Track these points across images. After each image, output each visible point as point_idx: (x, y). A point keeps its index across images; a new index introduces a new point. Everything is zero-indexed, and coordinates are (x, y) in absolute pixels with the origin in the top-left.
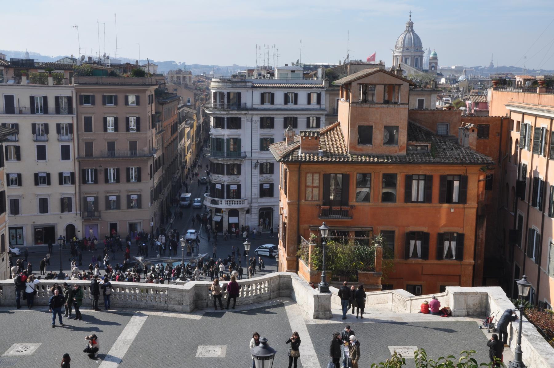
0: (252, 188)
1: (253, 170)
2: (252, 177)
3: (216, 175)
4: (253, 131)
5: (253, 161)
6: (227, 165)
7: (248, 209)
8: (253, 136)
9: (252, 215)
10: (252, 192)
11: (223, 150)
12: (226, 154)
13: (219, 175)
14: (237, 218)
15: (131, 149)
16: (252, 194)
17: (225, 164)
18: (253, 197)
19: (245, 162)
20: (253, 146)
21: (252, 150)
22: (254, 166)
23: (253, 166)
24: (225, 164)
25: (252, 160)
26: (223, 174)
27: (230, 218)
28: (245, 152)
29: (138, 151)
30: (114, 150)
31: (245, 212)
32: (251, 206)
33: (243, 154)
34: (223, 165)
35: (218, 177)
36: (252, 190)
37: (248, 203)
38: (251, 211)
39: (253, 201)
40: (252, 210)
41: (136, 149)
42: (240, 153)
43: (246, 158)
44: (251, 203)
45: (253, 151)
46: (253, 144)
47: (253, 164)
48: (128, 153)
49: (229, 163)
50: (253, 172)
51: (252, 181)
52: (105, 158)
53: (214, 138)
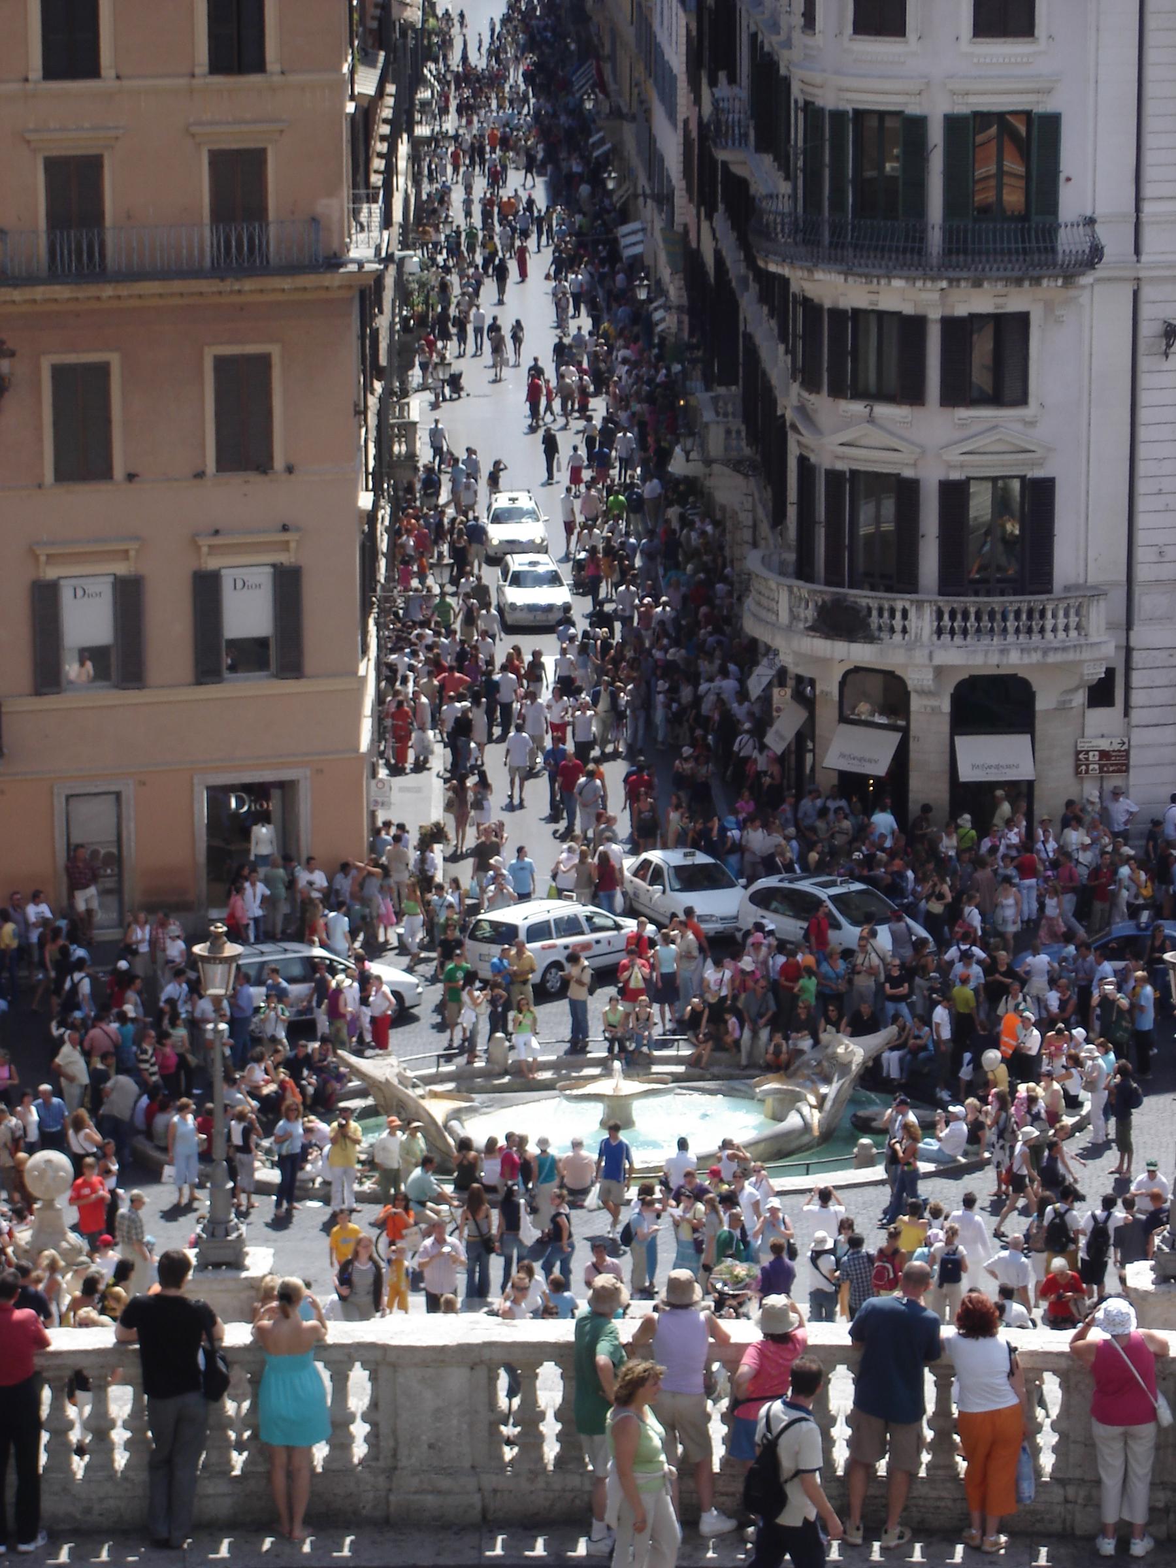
0: (1142, 504)
1: (1144, 363)
2: (1144, 415)
3: (857, 408)
4: (1151, 56)
5: (1147, 292)
6: (950, 325)
7: (1110, 672)
8: (1150, 89)
9: (1136, 716)
10: (1141, 537)
11: (919, 208)
12: (935, 239)
13: (883, 411)
14: (1028, 737)
15: (221, 214)
16: (1141, 554)
17: (934, 314)
18: (1143, 573)
19: (1084, 298)
20: (1149, 173)
21: (1138, 199)
22: (1158, 328)
23: (1149, 329)
24: (934, 314)
25: (1138, 279)
26: (912, 394)
27: (958, 740)
28: (1090, 222)
29: (272, 230)
30: (96, 217)
31: (1080, 698)
32: (1129, 650)
33: (1069, 241)
34: (914, 326)
35: (871, 420)
36: (1141, 520)
37: (1111, 626)
38: (1128, 688)
39: (1145, 603)
40: (1137, 678)
41: (258, 212)
42: (1050, 231)
43: (1101, 271)
44: (1129, 626)
45: (1148, 208)
46: (1149, 158)
47: (1146, 311)
48: (202, 250)
49: (961, 311)
50: (1144, 380)
51: (1143, 451)
52: (30, 280)
53: (838, 116)
